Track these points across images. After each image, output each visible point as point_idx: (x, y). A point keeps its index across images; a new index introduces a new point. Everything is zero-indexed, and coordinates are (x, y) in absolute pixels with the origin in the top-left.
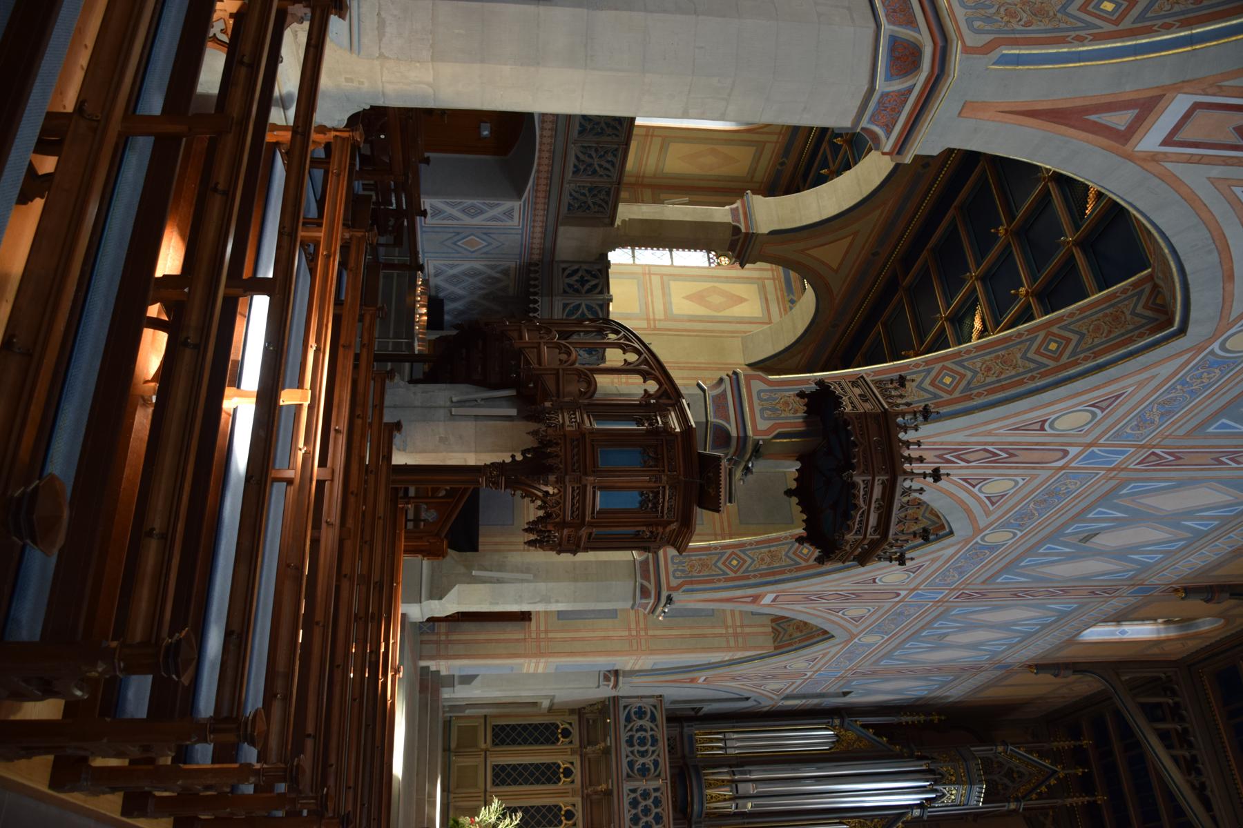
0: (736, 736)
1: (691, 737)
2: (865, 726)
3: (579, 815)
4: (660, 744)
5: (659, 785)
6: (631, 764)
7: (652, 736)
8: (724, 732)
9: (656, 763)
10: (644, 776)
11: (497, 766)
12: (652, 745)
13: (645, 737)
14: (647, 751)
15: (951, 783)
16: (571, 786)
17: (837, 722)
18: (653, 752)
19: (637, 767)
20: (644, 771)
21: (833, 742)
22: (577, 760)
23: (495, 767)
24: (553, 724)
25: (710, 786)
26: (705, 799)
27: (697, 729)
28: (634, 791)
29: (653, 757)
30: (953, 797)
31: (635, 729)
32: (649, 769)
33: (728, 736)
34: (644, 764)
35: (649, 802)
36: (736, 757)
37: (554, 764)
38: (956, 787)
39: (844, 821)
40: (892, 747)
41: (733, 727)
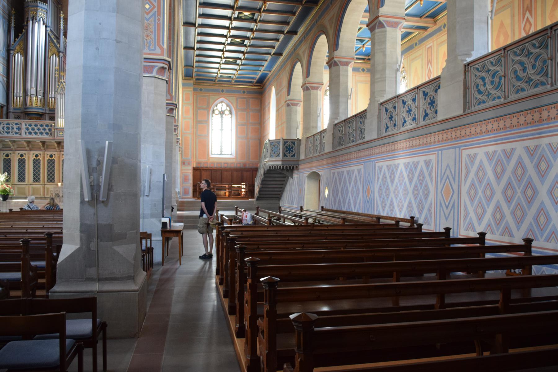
0: (15, 91)
1: (15, 109)
2: (15, 41)
3: (36, 153)
4: (9, 122)
5: (24, 124)
6: (16, 133)
7: (6, 124)
8: (14, 96)
9: (16, 124)
10: (20, 129)
11: (18, 180)
12: (9, 125)
13: (7, 127)
14: (12, 127)
15: (37, 14)
16: (27, 155)
17: (12, 52)
18: (12, 125)
19: (17, 131)
20: (19, 129)
21: (20, 55)
22: (17, 152)
23: (19, 181)
24: (4, 160)
25: (32, 104)
26: (37, 107)
27: (11, 106)
28: (26, 133)
29: (14, 125)
30: (43, 14)
31: (3, 131)
32: (18, 127)
33: (15, 95)
34: (17, 129)
35: (30, 128)
36: (23, 93)
37: (18, 160)
38: (38, 12)
39: (49, 56)
40: (23, 33)
41: (11, 92)
